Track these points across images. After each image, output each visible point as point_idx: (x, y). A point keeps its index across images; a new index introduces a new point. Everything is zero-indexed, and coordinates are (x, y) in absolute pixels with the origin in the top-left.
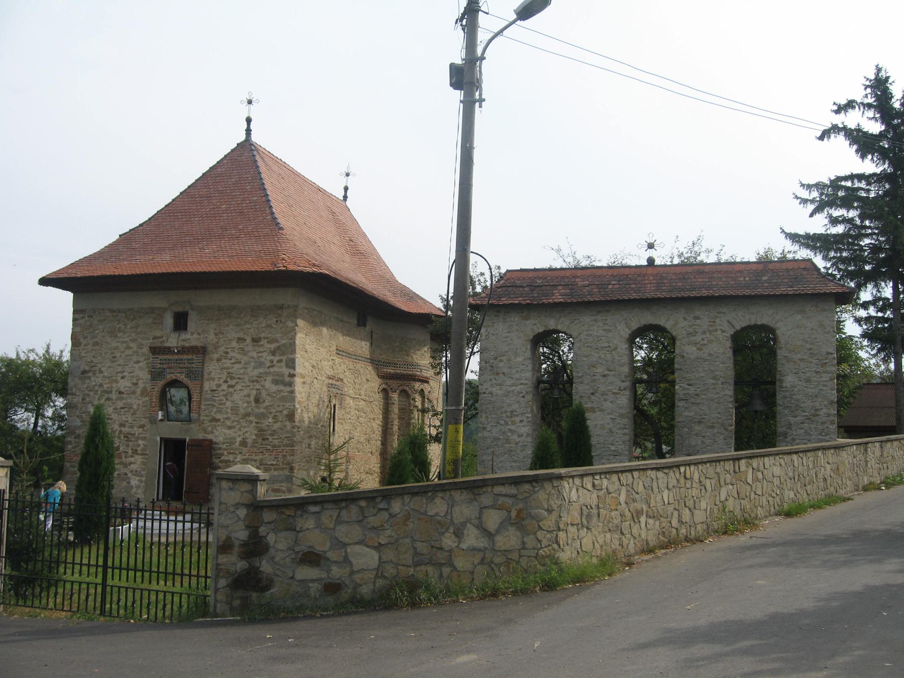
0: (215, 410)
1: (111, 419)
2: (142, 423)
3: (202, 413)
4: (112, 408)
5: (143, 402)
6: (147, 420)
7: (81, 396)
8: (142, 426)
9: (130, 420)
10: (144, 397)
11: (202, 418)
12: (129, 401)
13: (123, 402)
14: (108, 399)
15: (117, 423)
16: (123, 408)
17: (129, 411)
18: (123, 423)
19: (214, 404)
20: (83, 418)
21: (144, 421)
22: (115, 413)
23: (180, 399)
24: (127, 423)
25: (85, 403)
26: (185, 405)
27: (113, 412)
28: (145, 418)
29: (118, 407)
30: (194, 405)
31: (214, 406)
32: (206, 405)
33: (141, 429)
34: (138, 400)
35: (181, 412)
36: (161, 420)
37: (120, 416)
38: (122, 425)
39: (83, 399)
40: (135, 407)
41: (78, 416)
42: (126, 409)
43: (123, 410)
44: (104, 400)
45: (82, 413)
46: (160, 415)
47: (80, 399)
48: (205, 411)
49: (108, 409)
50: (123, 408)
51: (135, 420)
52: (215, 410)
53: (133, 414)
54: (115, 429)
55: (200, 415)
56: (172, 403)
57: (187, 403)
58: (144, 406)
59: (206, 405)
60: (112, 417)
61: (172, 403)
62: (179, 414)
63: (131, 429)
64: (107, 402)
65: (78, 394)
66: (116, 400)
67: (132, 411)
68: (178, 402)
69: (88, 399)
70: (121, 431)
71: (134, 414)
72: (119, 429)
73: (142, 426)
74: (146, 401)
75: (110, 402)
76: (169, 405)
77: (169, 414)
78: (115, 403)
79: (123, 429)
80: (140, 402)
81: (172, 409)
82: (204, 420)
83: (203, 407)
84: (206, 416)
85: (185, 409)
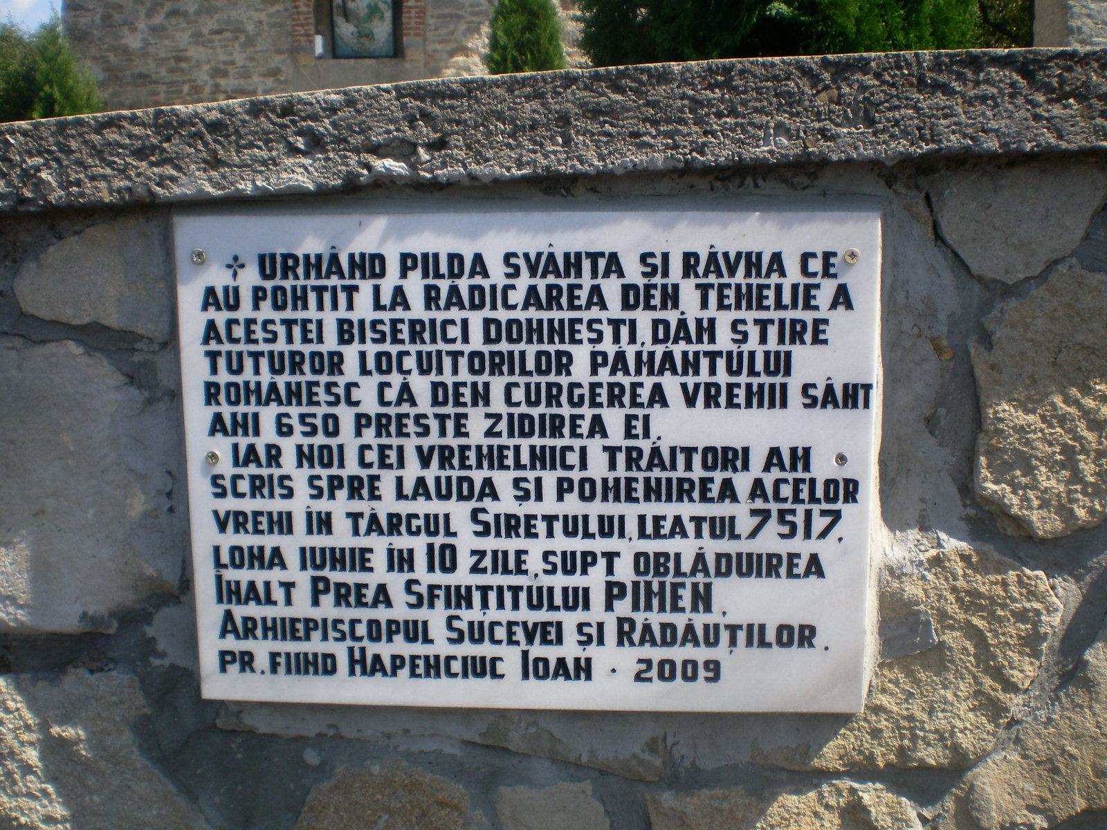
0: (463, 27)
1: (187, 59)
2: (273, 65)
3: (429, 35)
4: (189, 32)
5: (270, 16)
6: (283, 57)
7: (100, 10)
8: (274, 73)
9: (240, 59)
10: (272, 5)
11: (431, 47)
12: (234, 14)
13: (217, 16)
14: (174, 13)
15: (206, 67)
16: (219, 32)
17: (237, 38)
18: (222, 67)
19: (461, 13)
20: (108, 62)
21: (277, 60)
22: (197, 43)
23: (369, 6)
24: (230, 68)
25: (111, 26)
26: (382, 18)
27: (190, 43)
28: (280, 52)
29: (205, 31)
30: (410, 19)
31: (459, 17)
32: (439, 17)
33: (271, 79)
34: (256, 10)
35: (370, 36)
36: (320, 57)
37: (210, 51)
38: (218, 72)
39: (107, 17)
40: (250, 28)
41: (94, 58)
42: (227, 35)
43: (217, 37)
44: (163, 15)
45: (107, 50)
46: (319, 43)
47: (98, 19)
48: (436, 29)
49: (178, 35)
50: (219, 32)
51: (251, 59)
52: (463, 27)
53: (244, 45)
54: (200, 83)
55: (425, 40)
56: (346, 14)
57: (388, 15)
58: (274, 25)
59: (439, 17)
60: (188, 54)
61: (346, 14)
62: (363, 40)
63: (242, 81)
64: (174, 21)
65: (91, 7)
66: (198, 13)
67: (242, 38)
68: (363, 12)
69: (117, 17)
70: (217, 86)
71: (250, 42)
72: (211, 82)
73: (274, 73)
74: (279, 11)
75: (181, 20)
76: (339, 20)
77: (339, 42)
78: (195, 21)
79: (223, 82)
80: (263, 16)
81: (346, 30)
82: (434, 51)
83: (431, 21)
84: (441, 42)
85: (382, 30)
